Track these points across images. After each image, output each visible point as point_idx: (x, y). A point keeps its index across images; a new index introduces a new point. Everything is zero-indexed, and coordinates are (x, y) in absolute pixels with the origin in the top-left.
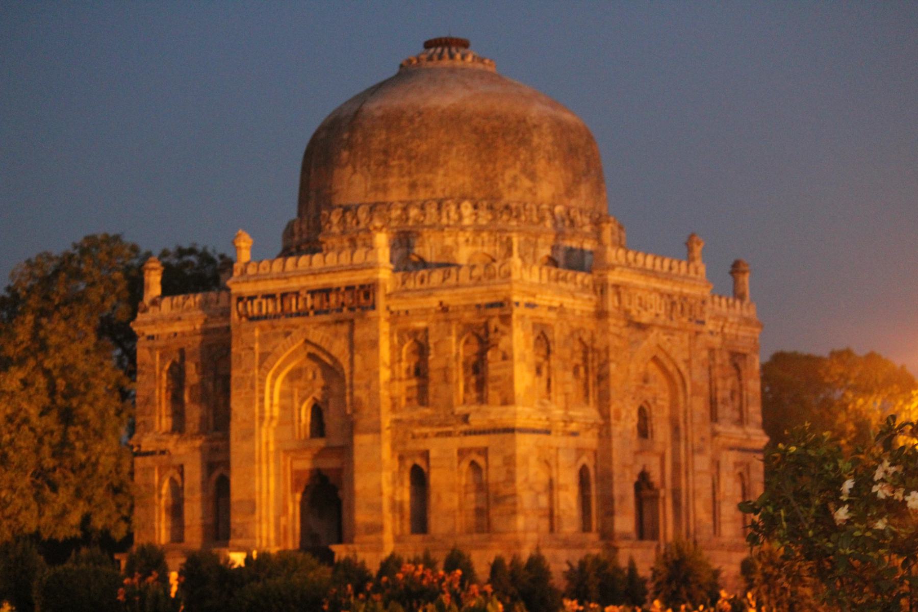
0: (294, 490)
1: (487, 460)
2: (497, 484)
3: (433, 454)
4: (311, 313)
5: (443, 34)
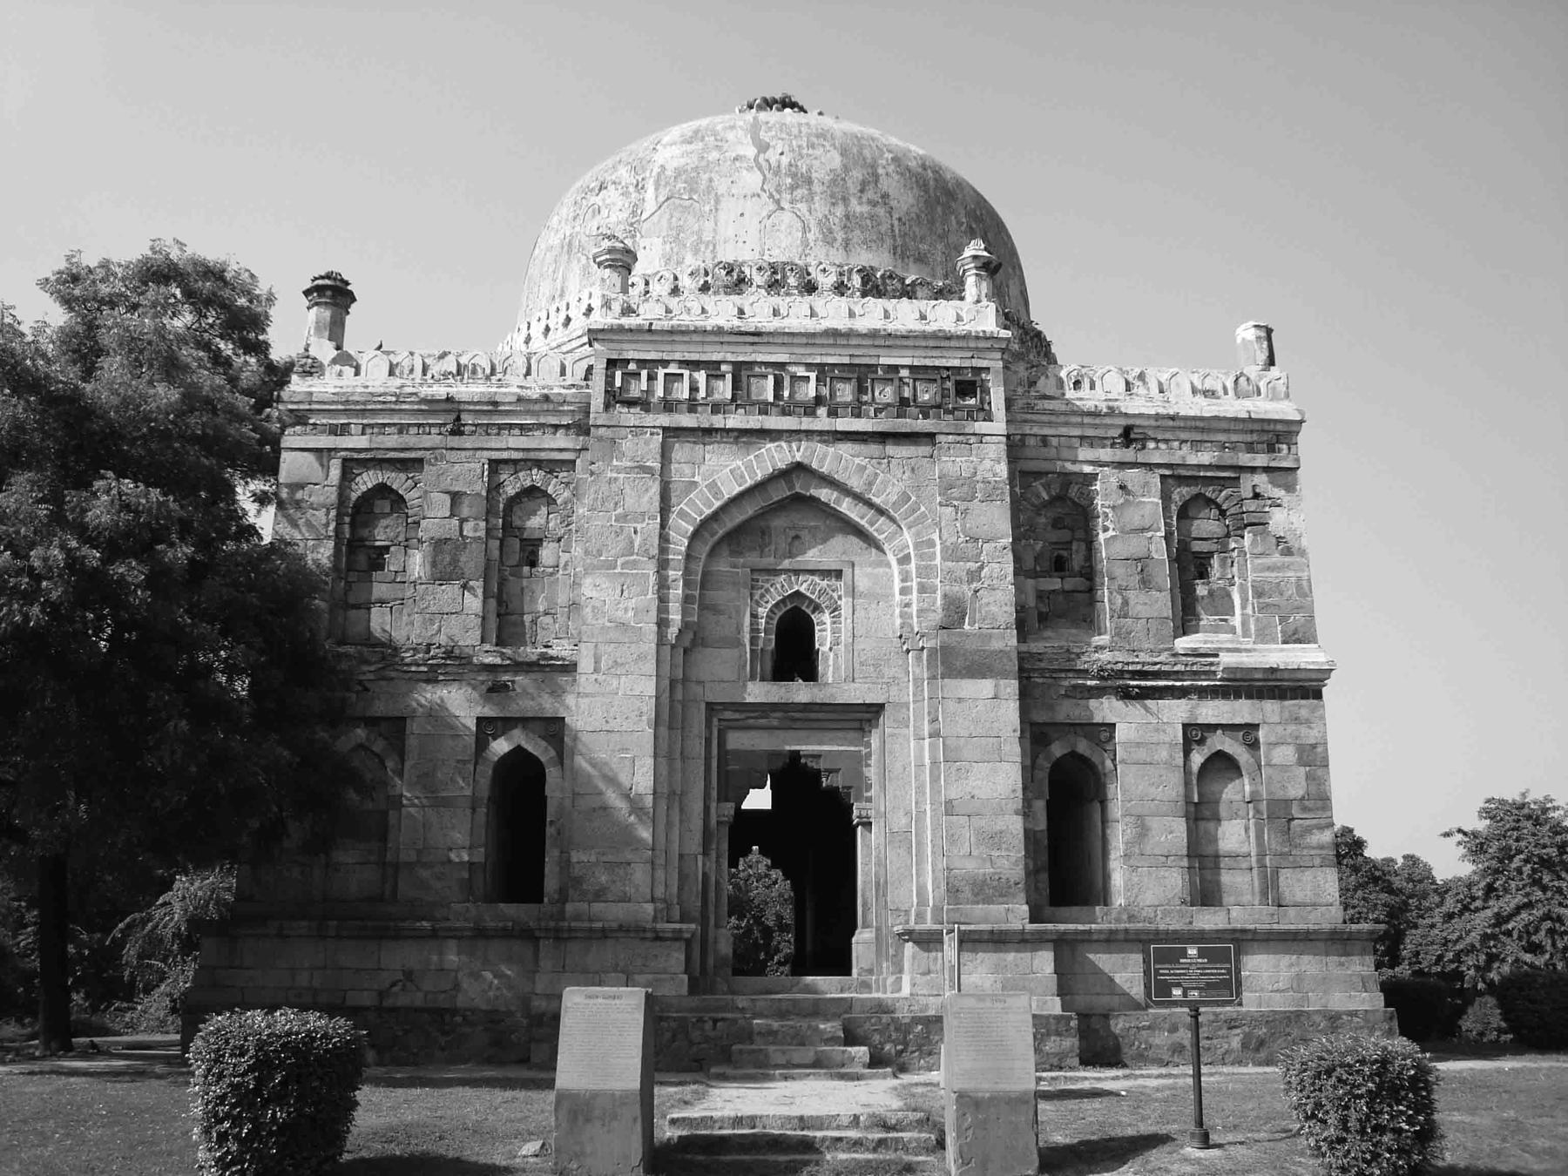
0: (723, 798)
2: (1288, 802)
3: (1120, 735)
4: (822, 411)
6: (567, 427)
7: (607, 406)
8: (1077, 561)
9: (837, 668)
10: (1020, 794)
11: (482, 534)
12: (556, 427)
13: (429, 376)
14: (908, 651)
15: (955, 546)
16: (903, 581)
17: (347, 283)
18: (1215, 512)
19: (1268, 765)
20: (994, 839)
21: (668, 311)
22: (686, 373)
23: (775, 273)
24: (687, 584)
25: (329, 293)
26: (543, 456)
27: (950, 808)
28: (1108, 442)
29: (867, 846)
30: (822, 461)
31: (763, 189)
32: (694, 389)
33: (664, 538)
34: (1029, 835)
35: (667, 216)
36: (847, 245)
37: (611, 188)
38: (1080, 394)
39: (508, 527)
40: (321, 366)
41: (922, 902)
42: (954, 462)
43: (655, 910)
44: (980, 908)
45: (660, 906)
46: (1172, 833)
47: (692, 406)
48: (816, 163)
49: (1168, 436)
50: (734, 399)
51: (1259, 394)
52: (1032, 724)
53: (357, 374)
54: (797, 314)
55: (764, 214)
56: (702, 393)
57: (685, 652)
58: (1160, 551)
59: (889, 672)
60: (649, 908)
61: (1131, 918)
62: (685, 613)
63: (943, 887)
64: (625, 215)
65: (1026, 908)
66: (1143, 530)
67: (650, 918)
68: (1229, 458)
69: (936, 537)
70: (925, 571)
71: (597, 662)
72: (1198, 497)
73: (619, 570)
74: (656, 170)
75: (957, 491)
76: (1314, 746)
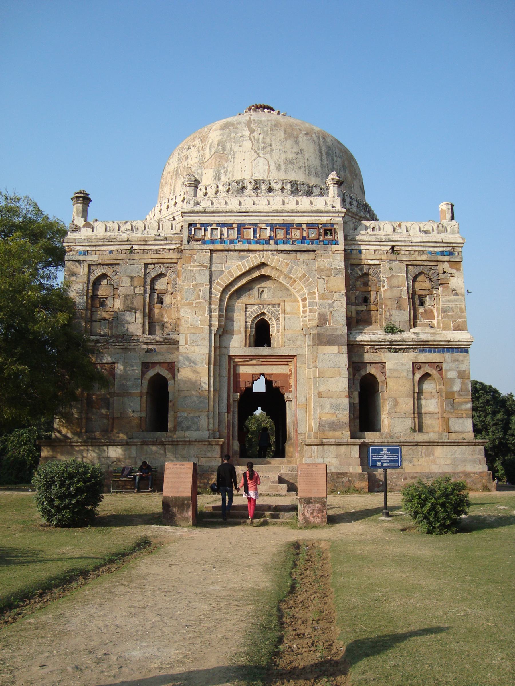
1: (441, 375)
2: (453, 393)
3: (388, 366)
5: (266, 104)
6: (174, 249)
7: (189, 242)
8: (372, 299)
9: (278, 342)
10: (347, 389)
11: (142, 292)
12: (170, 249)
13: (121, 231)
14: (305, 335)
15: (323, 294)
16: (303, 308)
17: (88, 195)
18: (428, 279)
19: (446, 378)
20: (337, 406)
21: (212, 203)
22: (219, 228)
23: (256, 184)
24: (220, 310)
25: (81, 199)
26: (165, 261)
27: (320, 395)
28: (385, 252)
29: (291, 409)
30: (272, 262)
31: (252, 149)
32: (222, 234)
33: (211, 292)
34: (351, 406)
35: (213, 162)
36: (285, 172)
37: (193, 148)
38: (374, 233)
39: (152, 289)
40: (79, 228)
41: (310, 431)
42: (323, 261)
44: (331, 433)
46: (407, 405)
47: (222, 241)
48: (274, 137)
49: (409, 248)
50: (237, 238)
51: (447, 231)
52: (354, 363)
53: (93, 231)
54: (262, 204)
55: (253, 159)
56: (225, 236)
57: (220, 336)
58: (405, 295)
59: (298, 343)
60: (206, 434)
61: (391, 437)
62: (219, 321)
63: (318, 425)
64: (197, 160)
65: (349, 433)
66: (399, 286)
67: (207, 437)
68: (433, 257)
69: (316, 291)
70: (311, 304)
71: (186, 341)
72: (421, 273)
73: (194, 306)
74: (210, 142)
75: (325, 273)
76: (464, 371)
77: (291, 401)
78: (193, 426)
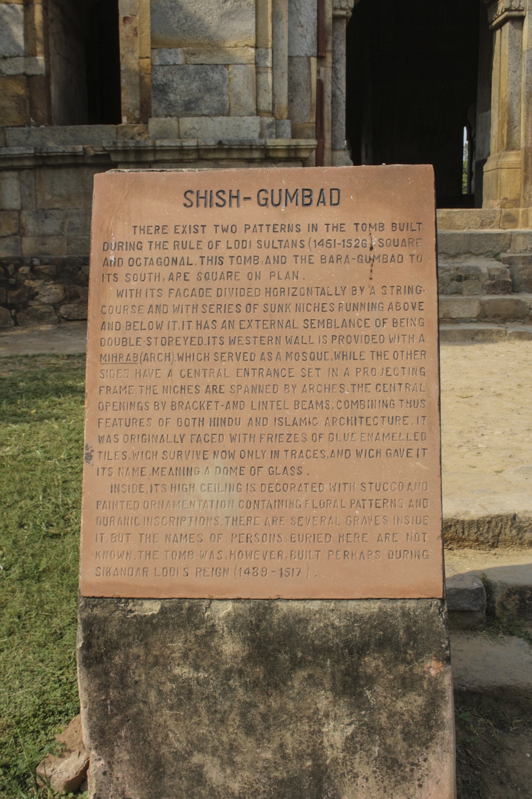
43: (261, 123)
45: (269, 120)
67: (256, 135)
77: (521, 19)
78: (207, 97)
